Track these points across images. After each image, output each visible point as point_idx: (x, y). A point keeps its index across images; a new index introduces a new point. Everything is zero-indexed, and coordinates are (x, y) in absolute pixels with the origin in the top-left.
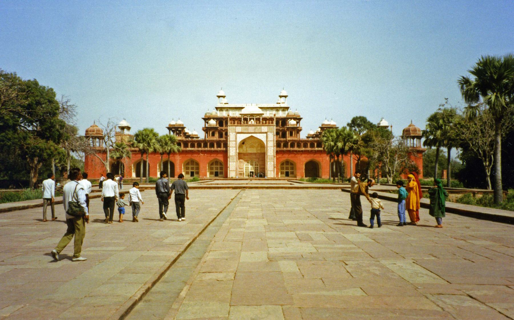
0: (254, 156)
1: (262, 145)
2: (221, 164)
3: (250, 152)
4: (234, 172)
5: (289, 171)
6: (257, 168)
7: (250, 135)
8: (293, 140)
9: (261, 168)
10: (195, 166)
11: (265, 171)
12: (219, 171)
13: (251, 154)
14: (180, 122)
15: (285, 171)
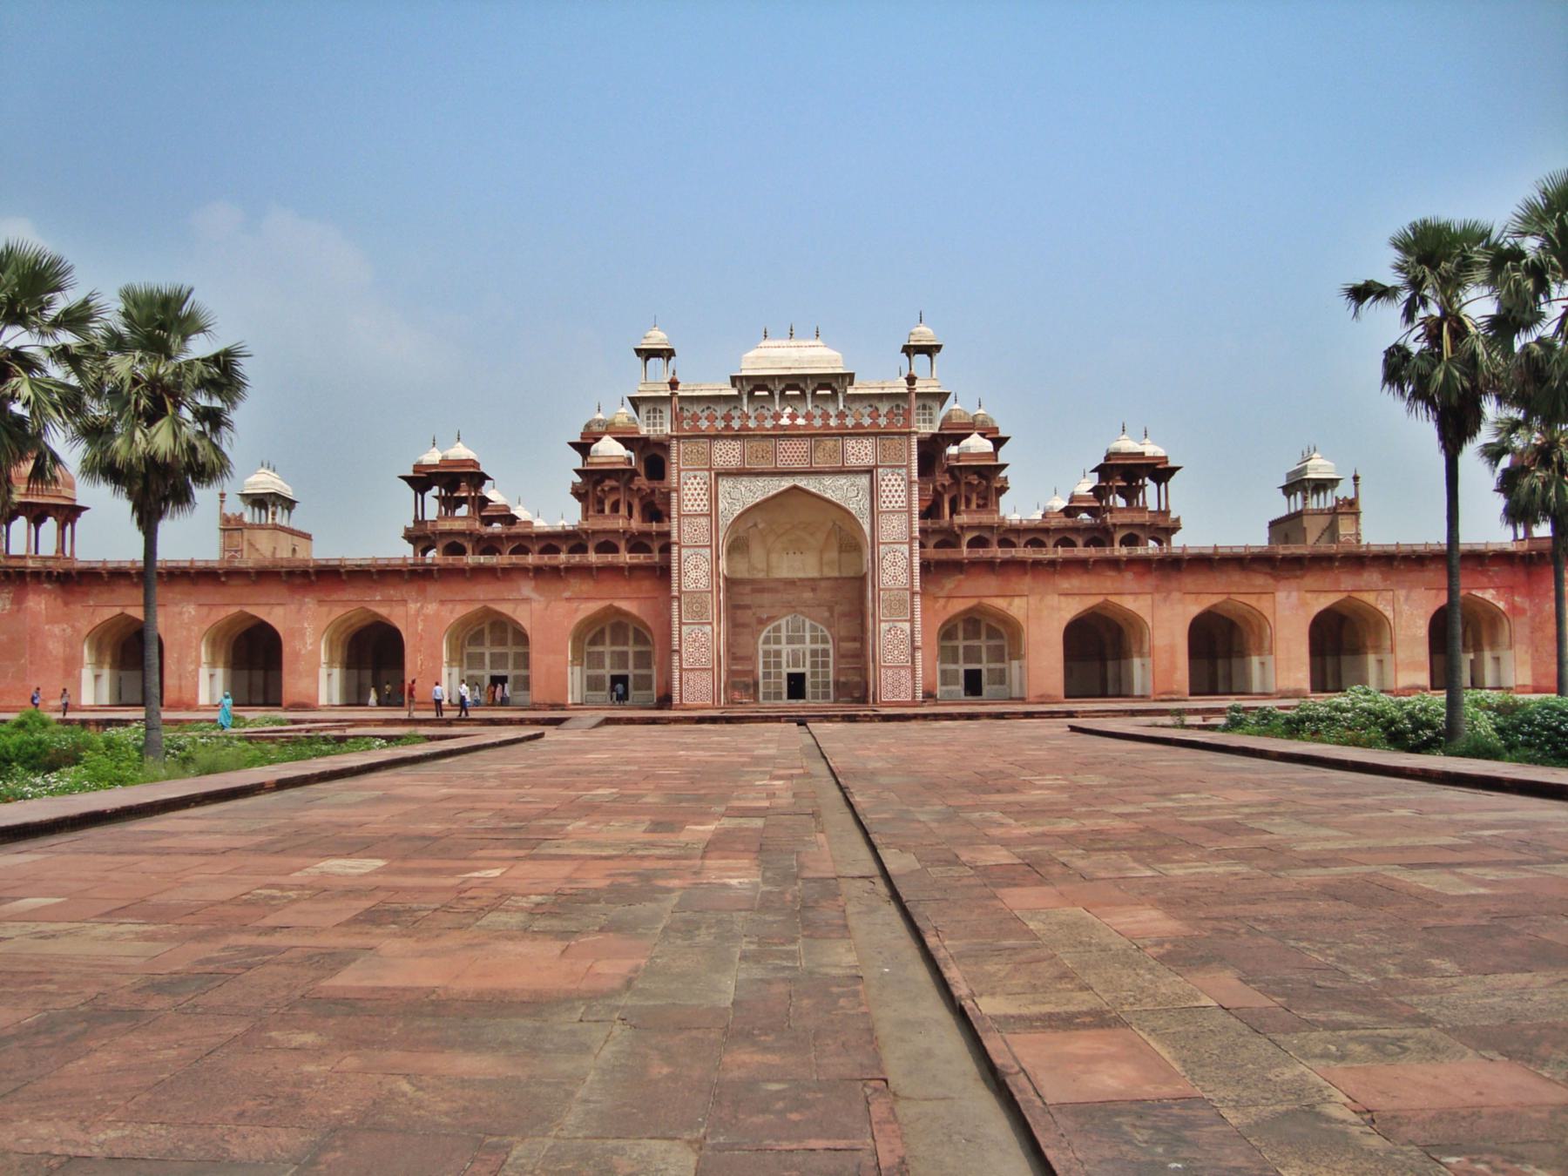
0: (808, 595)
1: (847, 536)
2: (641, 638)
3: (784, 573)
4: (707, 676)
5: (984, 666)
6: (825, 653)
7: (786, 483)
8: (979, 527)
9: (841, 656)
10: (511, 650)
11: (863, 671)
12: (631, 671)
13: (791, 583)
14: (460, 452)
15: (961, 668)
